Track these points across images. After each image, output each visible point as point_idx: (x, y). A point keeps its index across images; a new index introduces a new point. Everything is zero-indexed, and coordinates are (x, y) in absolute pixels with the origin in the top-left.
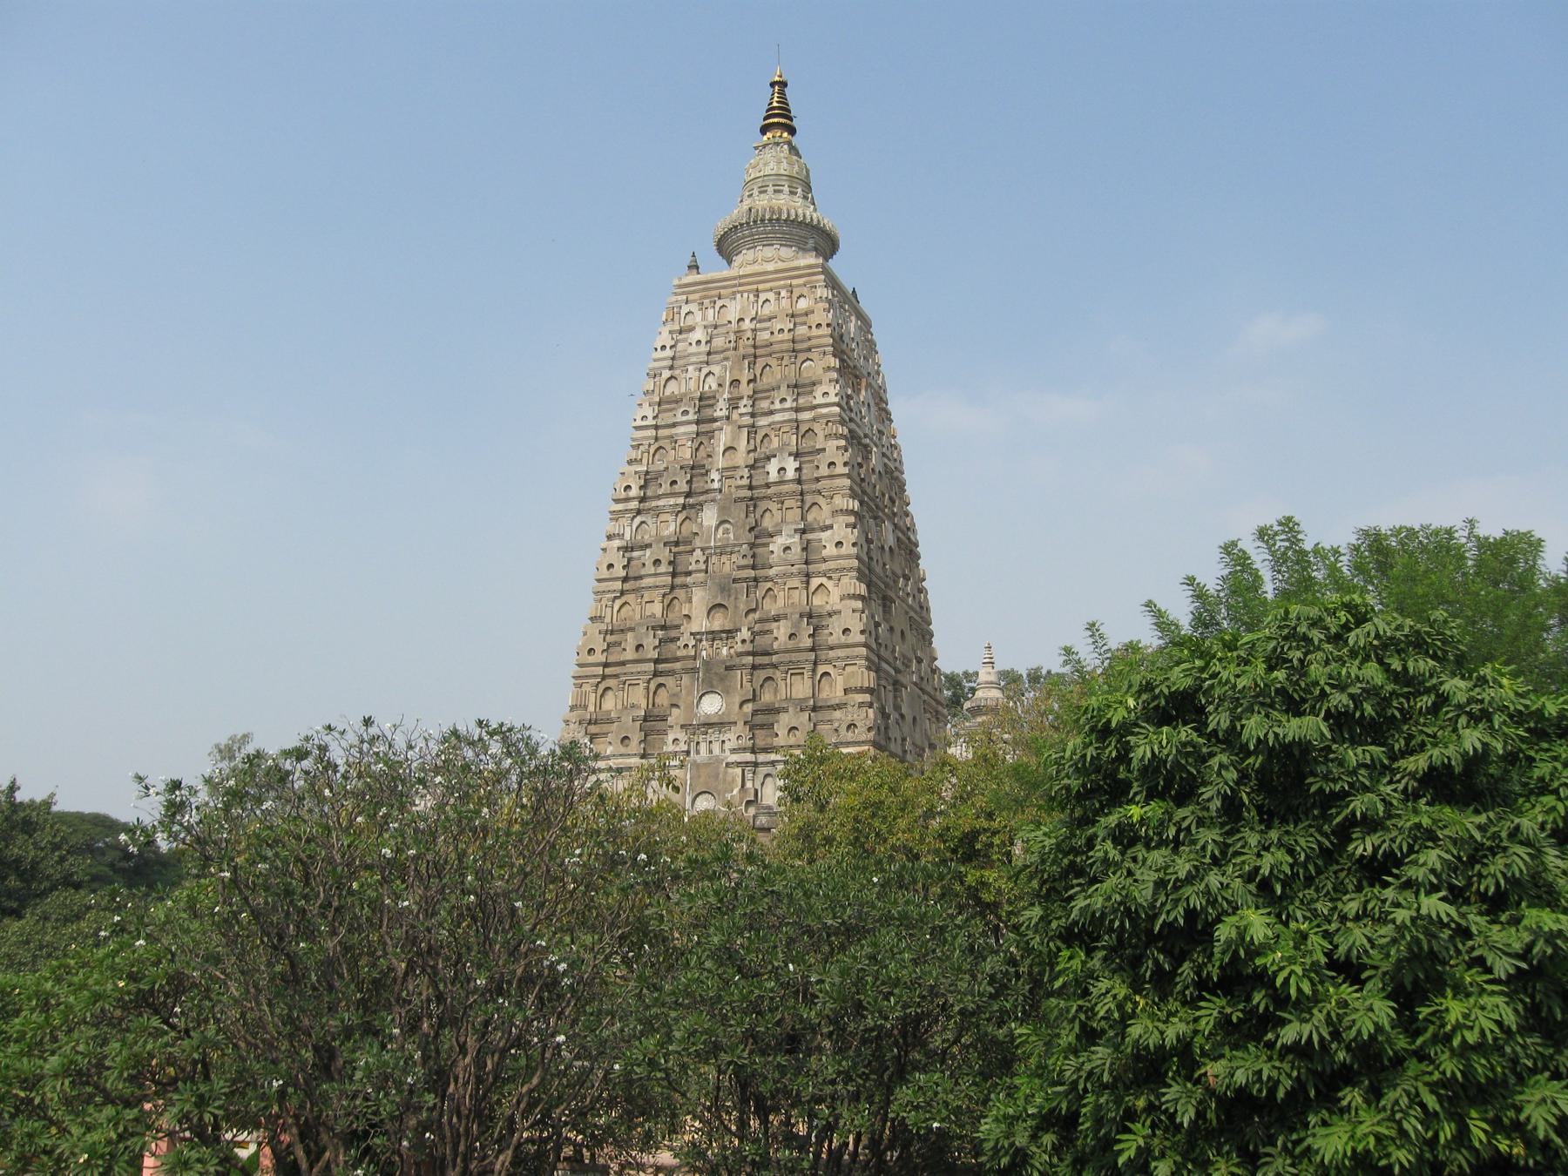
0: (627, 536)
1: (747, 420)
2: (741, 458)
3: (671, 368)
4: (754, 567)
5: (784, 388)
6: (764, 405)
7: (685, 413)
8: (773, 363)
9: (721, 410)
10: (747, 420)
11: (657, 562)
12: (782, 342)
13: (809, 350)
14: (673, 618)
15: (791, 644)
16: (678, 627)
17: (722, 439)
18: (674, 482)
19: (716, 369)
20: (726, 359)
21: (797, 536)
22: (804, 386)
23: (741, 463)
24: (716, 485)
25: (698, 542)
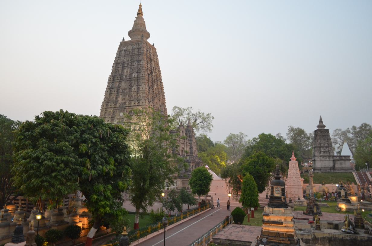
0: (110, 87)
1: (130, 67)
2: (128, 73)
3: (119, 58)
6: (133, 64)
7: (120, 65)
8: (135, 57)
9: (126, 65)
10: (130, 67)
11: (114, 91)
14: (117, 101)
15: (134, 105)
16: (117, 102)
17: (125, 70)
18: (118, 78)
19: (126, 58)
20: (127, 56)
21: (136, 87)
22: (139, 61)
23: (128, 74)
24: (124, 78)
25: (121, 88)
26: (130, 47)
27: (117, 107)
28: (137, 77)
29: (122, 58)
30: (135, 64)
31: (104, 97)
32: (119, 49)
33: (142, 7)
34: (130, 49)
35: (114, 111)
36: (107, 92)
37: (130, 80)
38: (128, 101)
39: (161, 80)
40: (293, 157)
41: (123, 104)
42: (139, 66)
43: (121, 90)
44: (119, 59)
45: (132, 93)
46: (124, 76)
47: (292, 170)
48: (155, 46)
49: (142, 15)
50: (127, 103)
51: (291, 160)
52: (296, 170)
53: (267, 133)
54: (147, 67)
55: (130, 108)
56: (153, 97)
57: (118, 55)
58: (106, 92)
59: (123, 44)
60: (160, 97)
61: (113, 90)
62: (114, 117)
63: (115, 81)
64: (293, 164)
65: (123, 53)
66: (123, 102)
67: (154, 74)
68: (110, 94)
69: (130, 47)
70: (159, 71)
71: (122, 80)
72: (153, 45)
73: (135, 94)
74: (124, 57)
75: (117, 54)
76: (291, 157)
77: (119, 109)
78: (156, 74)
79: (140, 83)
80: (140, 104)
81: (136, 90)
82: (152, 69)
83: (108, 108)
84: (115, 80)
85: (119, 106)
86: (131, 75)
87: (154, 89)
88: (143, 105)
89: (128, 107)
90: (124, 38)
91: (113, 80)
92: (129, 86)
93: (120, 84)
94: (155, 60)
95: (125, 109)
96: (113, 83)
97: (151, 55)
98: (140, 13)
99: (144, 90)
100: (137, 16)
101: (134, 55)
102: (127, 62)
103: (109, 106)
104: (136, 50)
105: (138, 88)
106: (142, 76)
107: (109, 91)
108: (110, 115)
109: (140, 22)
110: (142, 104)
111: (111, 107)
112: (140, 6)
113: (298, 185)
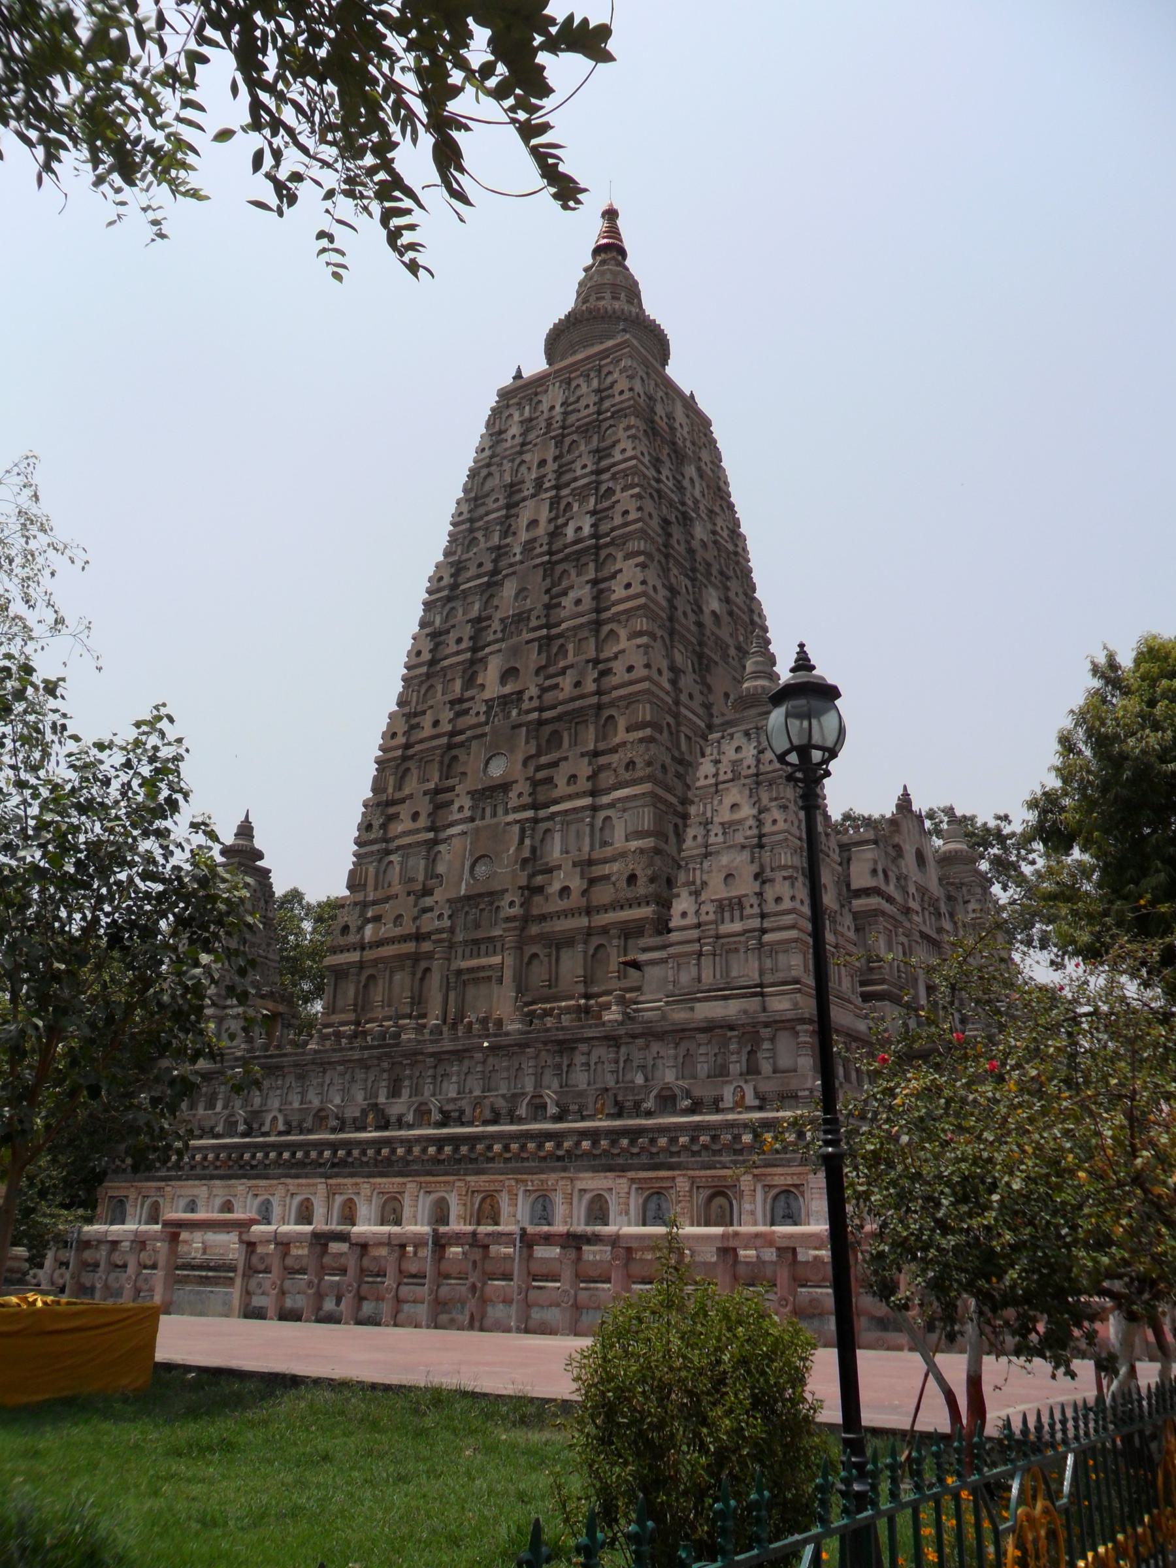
2: (541, 530)
15: (577, 692)
17: (525, 515)
24: (518, 557)
26: (554, 397)
28: (596, 536)
32: (489, 424)
34: (553, 408)
35: (454, 752)
41: (505, 701)
57: (487, 453)
59: (519, 395)
62: (452, 789)
66: (508, 689)
69: (554, 397)
77: (484, 735)
85: (483, 718)
92: (548, 591)
96: (450, 605)
97: (679, 443)
110: (627, 677)
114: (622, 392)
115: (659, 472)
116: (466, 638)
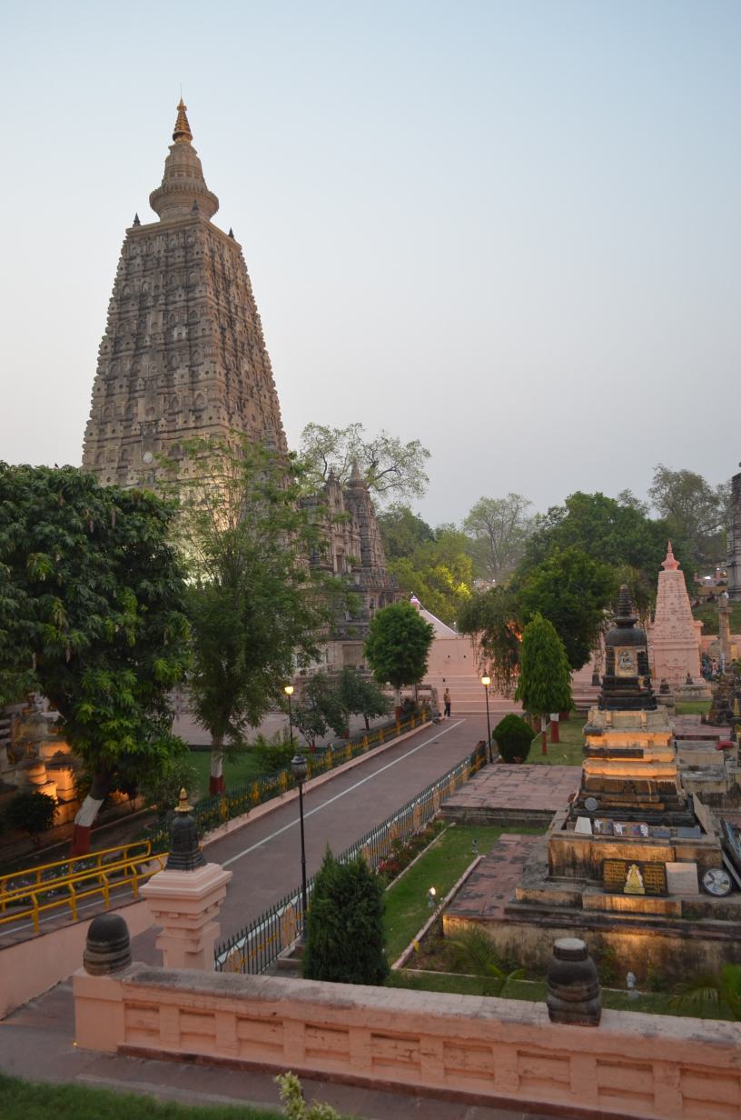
0: (107, 373)
1: (163, 307)
3: (126, 280)
4: (168, 387)
5: (180, 289)
6: (171, 298)
7: (133, 305)
8: (176, 274)
10: (163, 307)
11: (121, 386)
12: (180, 263)
13: (192, 267)
14: (130, 416)
16: (131, 420)
17: (150, 319)
18: (128, 343)
19: (148, 279)
20: (152, 274)
21: (187, 369)
24: (148, 344)
25: (140, 375)
26: (158, 245)
27: (134, 436)
28: (189, 340)
29: (136, 282)
30: (177, 299)
31: (90, 407)
32: (124, 251)
33: (186, 112)
34: (159, 252)
35: (125, 447)
36: (99, 390)
37: (167, 348)
38: (166, 416)
39: (260, 343)
40: (670, 558)
41: (149, 424)
42: (191, 304)
43: (140, 381)
44: (127, 285)
45: (176, 389)
46: (148, 339)
47: (668, 597)
48: (238, 239)
49: (190, 137)
50: (163, 421)
51: (663, 569)
52: (680, 596)
53: (590, 491)
54: (216, 307)
55: (172, 435)
56: (240, 399)
57: (124, 272)
58: (96, 389)
59: (137, 236)
60: (262, 398)
61: (117, 383)
62: (126, 467)
63: (120, 355)
64: (671, 580)
65: (139, 265)
66: (150, 418)
67: (238, 327)
68: (109, 395)
69: (158, 245)
70: (255, 317)
71: (141, 351)
72: (231, 235)
73: (186, 393)
74: (144, 276)
75: (120, 268)
76: (665, 559)
77: (140, 441)
78: (245, 326)
79: (198, 358)
80: (204, 423)
81: (187, 379)
82: (233, 310)
83: (106, 440)
84: (121, 352)
85: (138, 432)
86: (168, 332)
87: (243, 372)
88: (211, 425)
89: (165, 435)
90: (137, 217)
91: (116, 352)
92: (166, 367)
93: (135, 362)
94: (240, 282)
95: (158, 439)
97: (226, 268)
98: (182, 133)
99: (212, 379)
100: (173, 143)
101: (174, 270)
102: (153, 294)
103: (109, 435)
104: (177, 253)
105: (193, 374)
106: (204, 336)
107: (103, 387)
108: (113, 461)
109: (184, 161)
110: (209, 422)
111: (115, 435)
112: (182, 108)
113: (686, 640)
114: (198, 253)
115: (218, 299)
116: (124, 386)
